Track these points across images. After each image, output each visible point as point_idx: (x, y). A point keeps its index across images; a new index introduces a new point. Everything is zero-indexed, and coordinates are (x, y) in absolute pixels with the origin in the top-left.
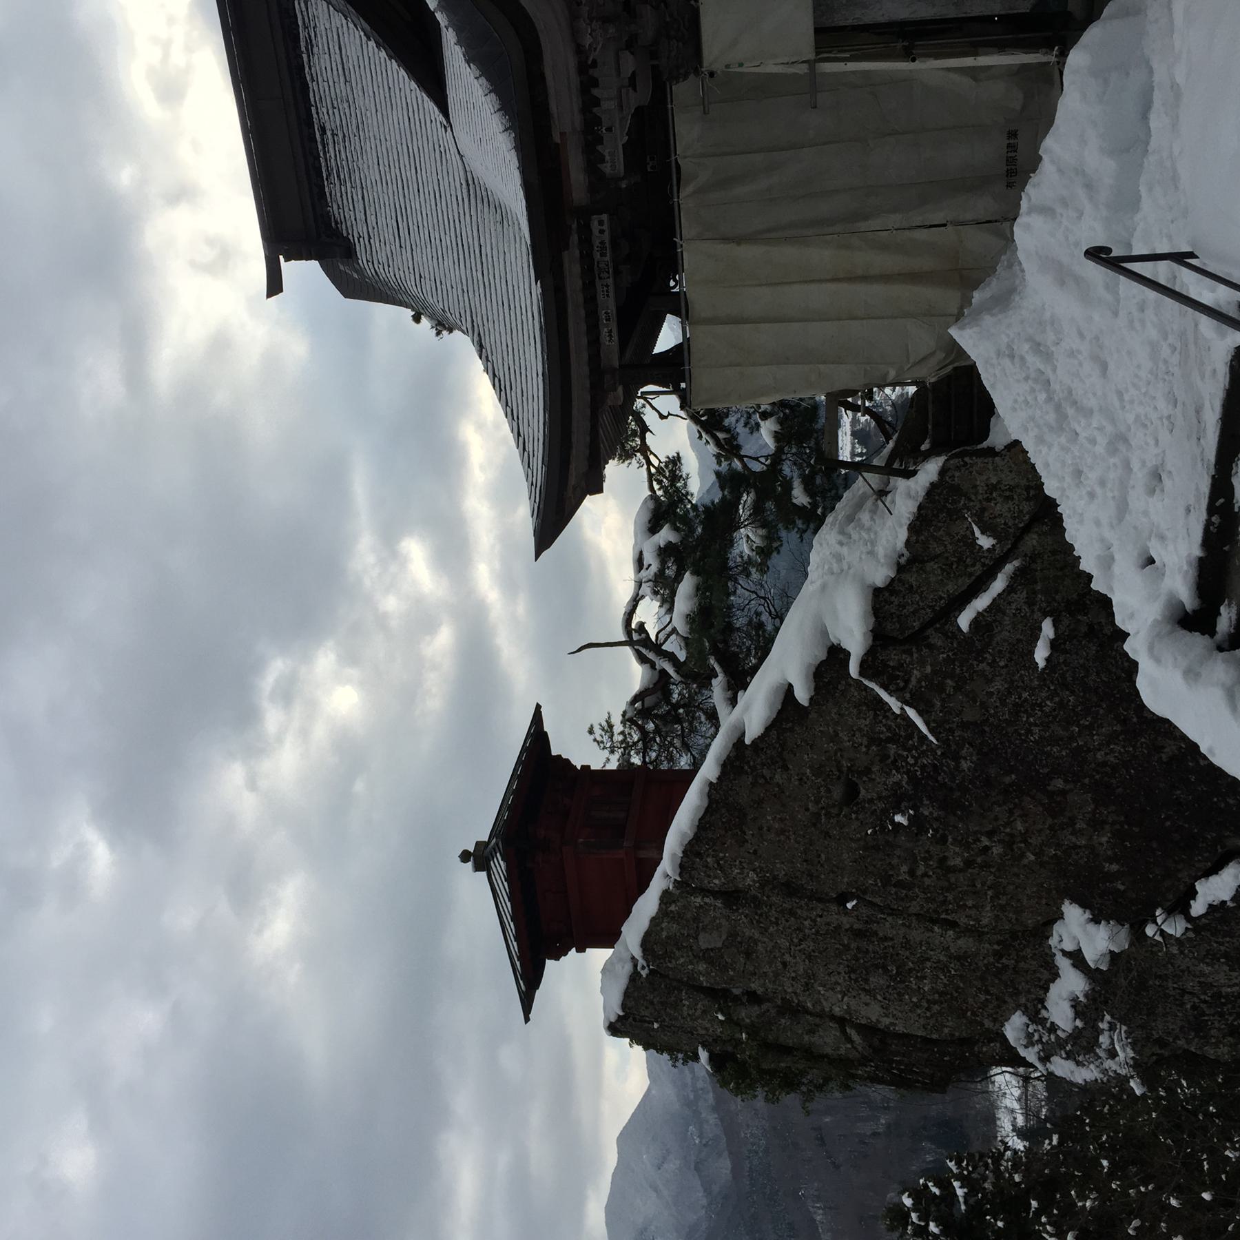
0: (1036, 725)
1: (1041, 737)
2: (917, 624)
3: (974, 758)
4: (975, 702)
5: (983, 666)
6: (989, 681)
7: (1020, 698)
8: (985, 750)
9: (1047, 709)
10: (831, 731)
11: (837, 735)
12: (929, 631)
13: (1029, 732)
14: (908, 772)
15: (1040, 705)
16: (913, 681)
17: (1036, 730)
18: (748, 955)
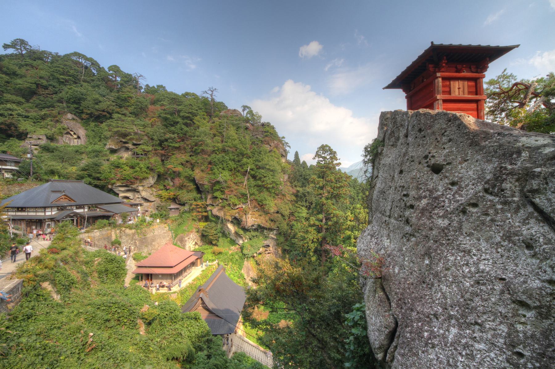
0: (455, 259)
1: (449, 260)
2: (537, 201)
3: (442, 225)
4: (474, 230)
5: (498, 239)
6: (487, 240)
7: (474, 255)
8: (446, 231)
9: (464, 268)
10: (468, 158)
11: (466, 161)
12: (530, 209)
13: (453, 255)
14: (443, 195)
15: (467, 265)
16: (491, 198)
17: (452, 258)
18: (392, 145)
